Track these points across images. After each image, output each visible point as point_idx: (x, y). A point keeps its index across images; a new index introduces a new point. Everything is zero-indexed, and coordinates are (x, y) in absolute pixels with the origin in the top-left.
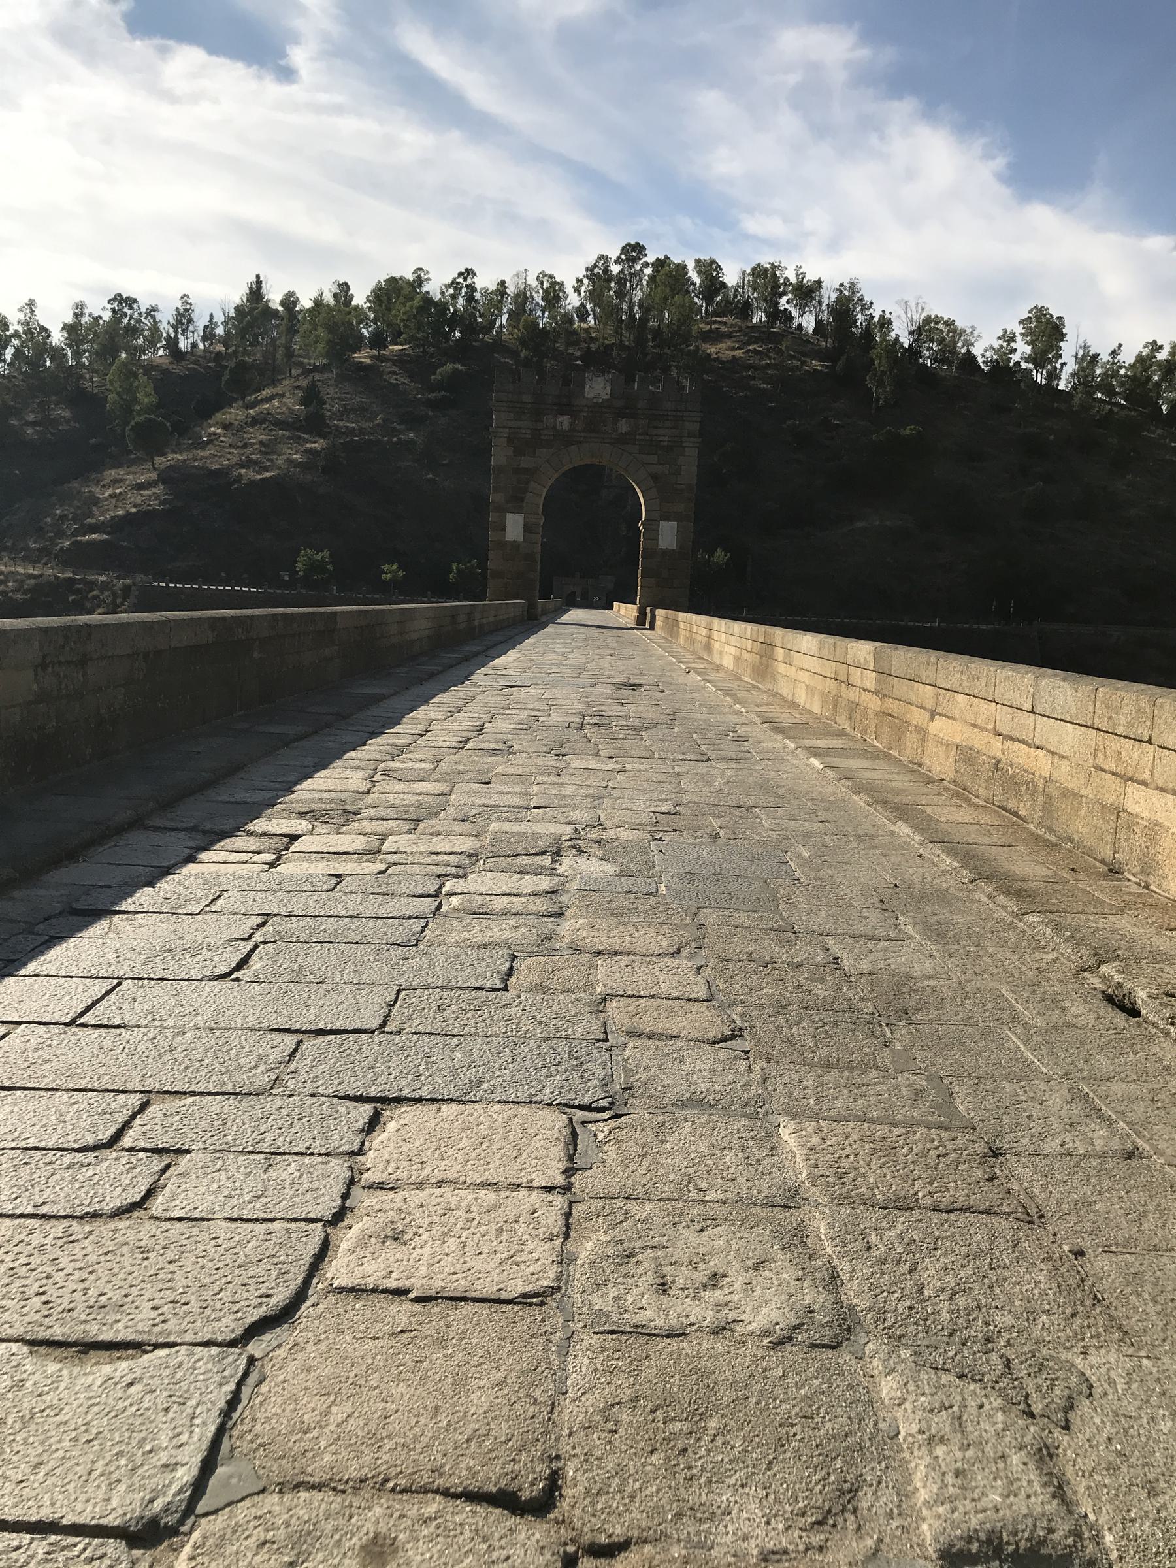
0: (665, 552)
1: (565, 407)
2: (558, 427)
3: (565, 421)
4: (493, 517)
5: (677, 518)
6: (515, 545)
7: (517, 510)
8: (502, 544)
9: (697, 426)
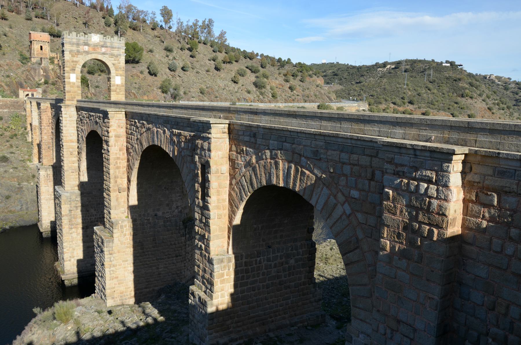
0: (117, 85)
1: (86, 44)
2: (84, 49)
3: (86, 48)
4: (66, 75)
5: (121, 76)
6: (74, 83)
7: (74, 73)
8: (69, 83)
9: (124, 51)
